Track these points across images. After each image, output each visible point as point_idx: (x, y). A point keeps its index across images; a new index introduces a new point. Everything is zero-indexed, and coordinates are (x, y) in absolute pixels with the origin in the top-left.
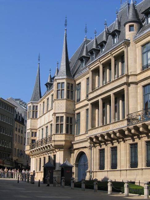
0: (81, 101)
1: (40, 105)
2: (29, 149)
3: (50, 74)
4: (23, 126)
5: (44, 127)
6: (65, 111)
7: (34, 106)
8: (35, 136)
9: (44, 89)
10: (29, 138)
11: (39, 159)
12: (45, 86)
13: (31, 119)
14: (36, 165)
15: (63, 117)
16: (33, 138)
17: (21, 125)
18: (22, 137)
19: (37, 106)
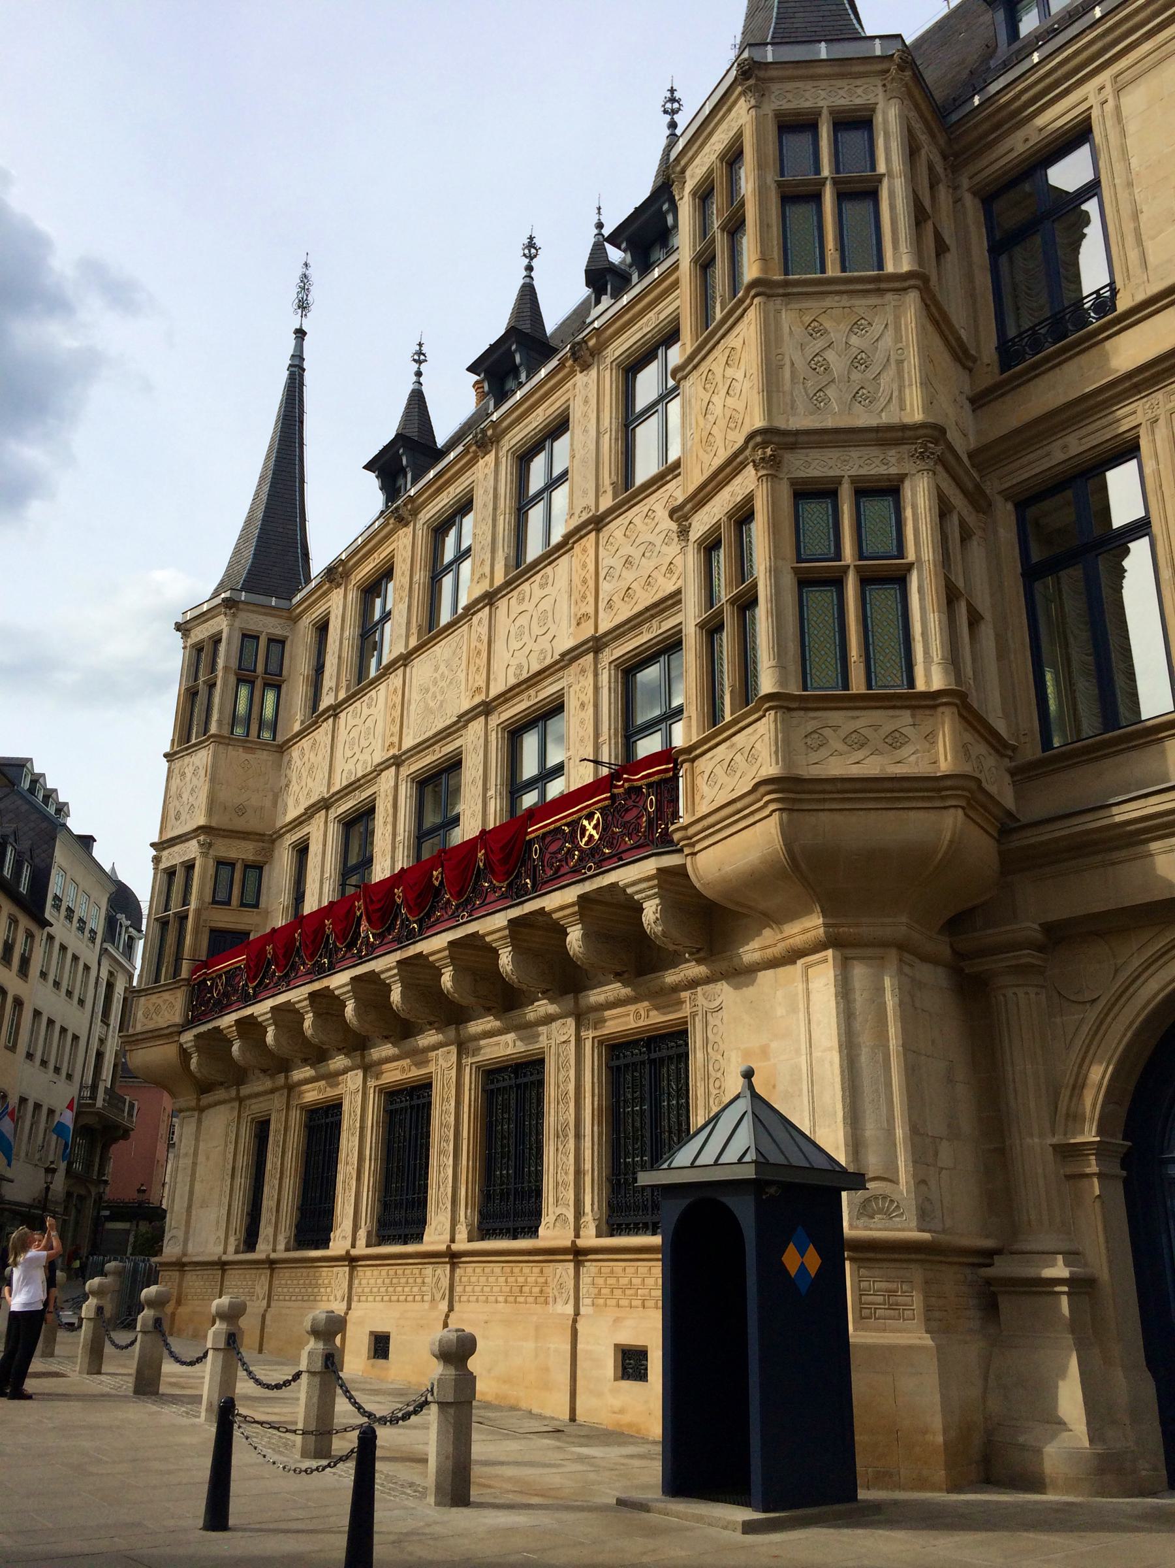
0: (1123, 303)
1: (322, 628)
2: (177, 1019)
3: (409, 387)
4: (34, 928)
5: (387, 780)
6: (914, 412)
7: (249, 638)
8: (242, 905)
9: (340, 510)
10: (183, 918)
11: (296, 1117)
12: (372, 481)
13: (218, 739)
14: (242, 1181)
15: (889, 490)
16: (225, 919)
17: (24, 922)
18: (18, 1003)
19: (278, 643)
